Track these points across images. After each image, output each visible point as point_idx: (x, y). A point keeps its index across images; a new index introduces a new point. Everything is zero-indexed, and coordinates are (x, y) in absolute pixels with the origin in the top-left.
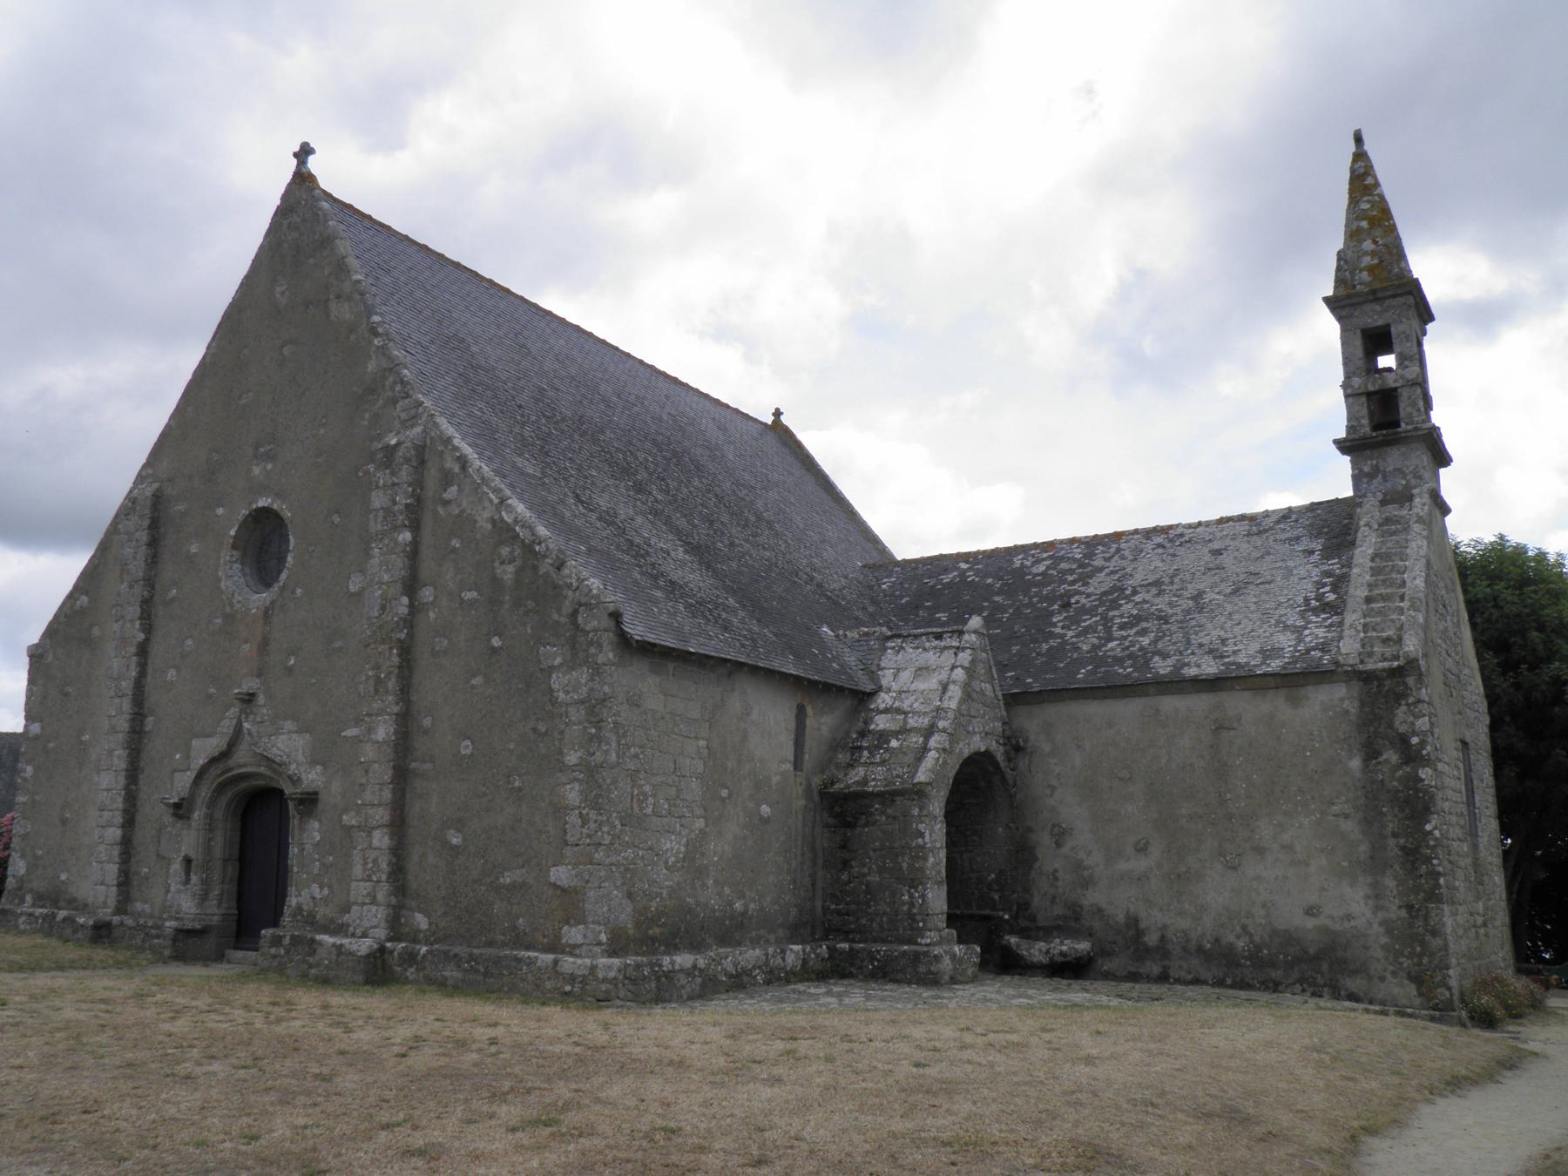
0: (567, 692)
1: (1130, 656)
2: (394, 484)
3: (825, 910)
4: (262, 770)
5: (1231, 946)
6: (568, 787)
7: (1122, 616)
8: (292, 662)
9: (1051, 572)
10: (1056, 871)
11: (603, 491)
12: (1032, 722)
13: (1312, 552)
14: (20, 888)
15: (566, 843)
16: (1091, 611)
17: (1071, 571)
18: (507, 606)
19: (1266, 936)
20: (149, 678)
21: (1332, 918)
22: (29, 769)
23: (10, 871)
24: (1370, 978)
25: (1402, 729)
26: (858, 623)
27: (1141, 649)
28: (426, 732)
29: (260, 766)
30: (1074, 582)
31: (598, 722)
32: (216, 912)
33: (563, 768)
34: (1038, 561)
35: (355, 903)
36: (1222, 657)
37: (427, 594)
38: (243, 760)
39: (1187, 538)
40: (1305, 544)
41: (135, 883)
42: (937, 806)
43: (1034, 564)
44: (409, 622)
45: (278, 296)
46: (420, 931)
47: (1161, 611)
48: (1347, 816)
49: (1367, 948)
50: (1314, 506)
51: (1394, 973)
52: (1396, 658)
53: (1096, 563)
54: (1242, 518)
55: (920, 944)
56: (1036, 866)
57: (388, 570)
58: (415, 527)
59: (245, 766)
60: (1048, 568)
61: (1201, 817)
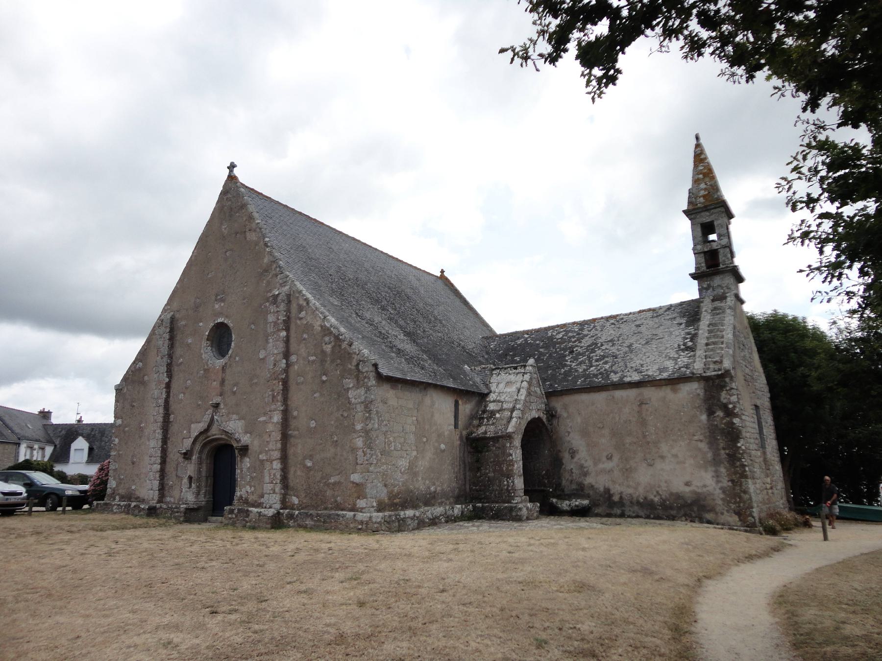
0: (356, 399)
1: (601, 374)
2: (278, 311)
3: (471, 489)
4: (223, 436)
5: (652, 501)
6: (358, 439)
7: (596, 356)
8: (235, 389)
9: (565, 337)
10: (572, 469)
11: (368, 311)
12: (558, 404)
13: (681, 324)
14: (113, 493)
15: (357, 464)
16: (583, 354)
17: (574, 337)
18: (328, 362)
19: (668, 496)
20: (171, 398)
21: (697, 486)
22: (117, 440)
23: (108, 486)
24: (716, 513)
25: (725, 401)
26: (481, 363)
27: (605, 370)
28: (295, 418)
29: (222, 435)
30: (575, 341)
31: (370, 411)
32: (203, 500)
33: (355, 431)
34: (559, 333)
35: (266, 493)
36: (641, 372)
37: (293, 358)
38: (214, 432)
39: (625, 320)
40: (678, 320)
41: (167, 489)
42: (517, 442)
43: (557, 334)
44: (286, 370)
46: (295, 505)
47: (614, 353)
48: (701, 441)
49: (714, 500)
50: (682, 304)
51: (728, 511)
52: (720, 370)
53: (584, 333)
54: (649, 310)
55: (513, 503)
56: (564, 467)
57: (276, 348)
58: (287, 329)
59: (215, 435)
60: (563, 336)
61: (635, 443)
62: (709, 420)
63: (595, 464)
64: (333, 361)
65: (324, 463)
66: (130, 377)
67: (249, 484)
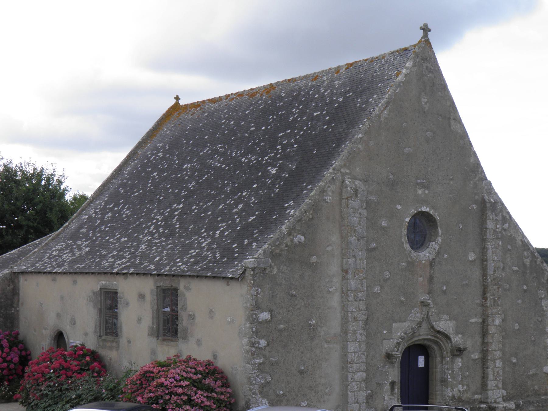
8: (445, 288)
45: (423, 103)
57: (496, 256)
67: (461, 382)
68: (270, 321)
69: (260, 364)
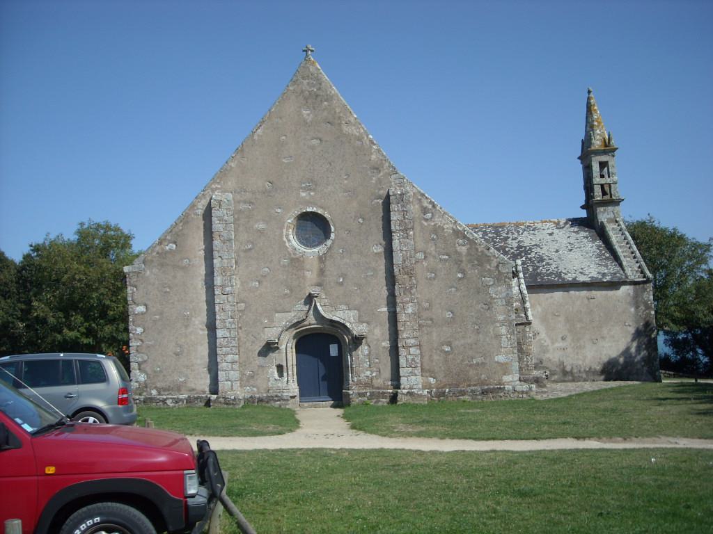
0: (497, 295)
5: (595, 369)
8: (341, 280)
22: (139, 330)
45: (305, 116)
62: (635, 310)
63: (553, 343)
64: (470, 261)
65: (465, 348)
66: (154, 259)
68: (145, 313)
69: (138, 346)
